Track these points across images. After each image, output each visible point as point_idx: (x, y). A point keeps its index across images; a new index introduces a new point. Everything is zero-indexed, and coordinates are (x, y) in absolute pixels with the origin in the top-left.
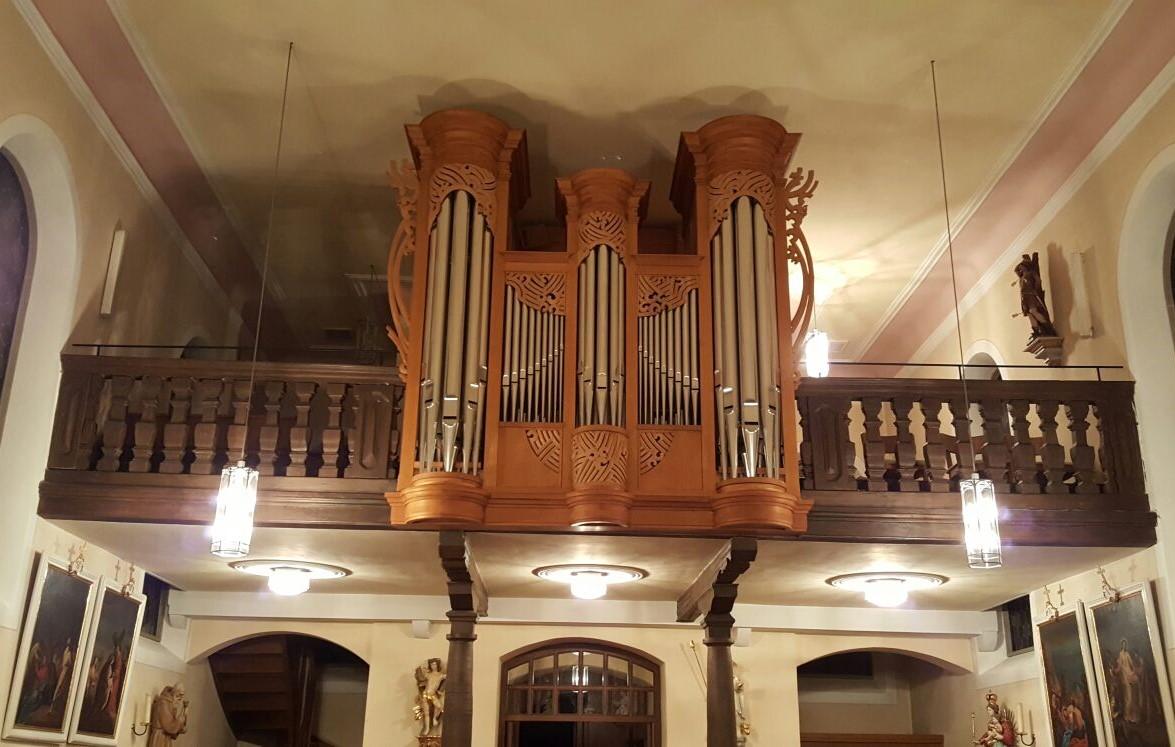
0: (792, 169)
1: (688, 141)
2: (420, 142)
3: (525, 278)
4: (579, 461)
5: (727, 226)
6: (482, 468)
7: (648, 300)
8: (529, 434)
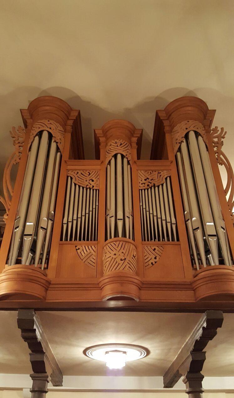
0: (213, 127)
1: (160, 114)
2: (27, 116)
3: (78, 173)
4: (108, 260)
5: (184, 145)
6: (47, 268)
7: (144, 181)
8: (77, 248)
